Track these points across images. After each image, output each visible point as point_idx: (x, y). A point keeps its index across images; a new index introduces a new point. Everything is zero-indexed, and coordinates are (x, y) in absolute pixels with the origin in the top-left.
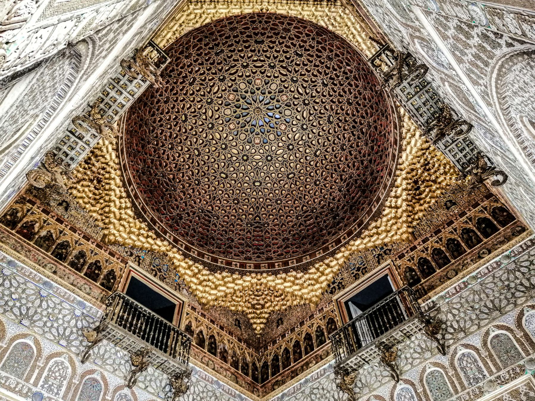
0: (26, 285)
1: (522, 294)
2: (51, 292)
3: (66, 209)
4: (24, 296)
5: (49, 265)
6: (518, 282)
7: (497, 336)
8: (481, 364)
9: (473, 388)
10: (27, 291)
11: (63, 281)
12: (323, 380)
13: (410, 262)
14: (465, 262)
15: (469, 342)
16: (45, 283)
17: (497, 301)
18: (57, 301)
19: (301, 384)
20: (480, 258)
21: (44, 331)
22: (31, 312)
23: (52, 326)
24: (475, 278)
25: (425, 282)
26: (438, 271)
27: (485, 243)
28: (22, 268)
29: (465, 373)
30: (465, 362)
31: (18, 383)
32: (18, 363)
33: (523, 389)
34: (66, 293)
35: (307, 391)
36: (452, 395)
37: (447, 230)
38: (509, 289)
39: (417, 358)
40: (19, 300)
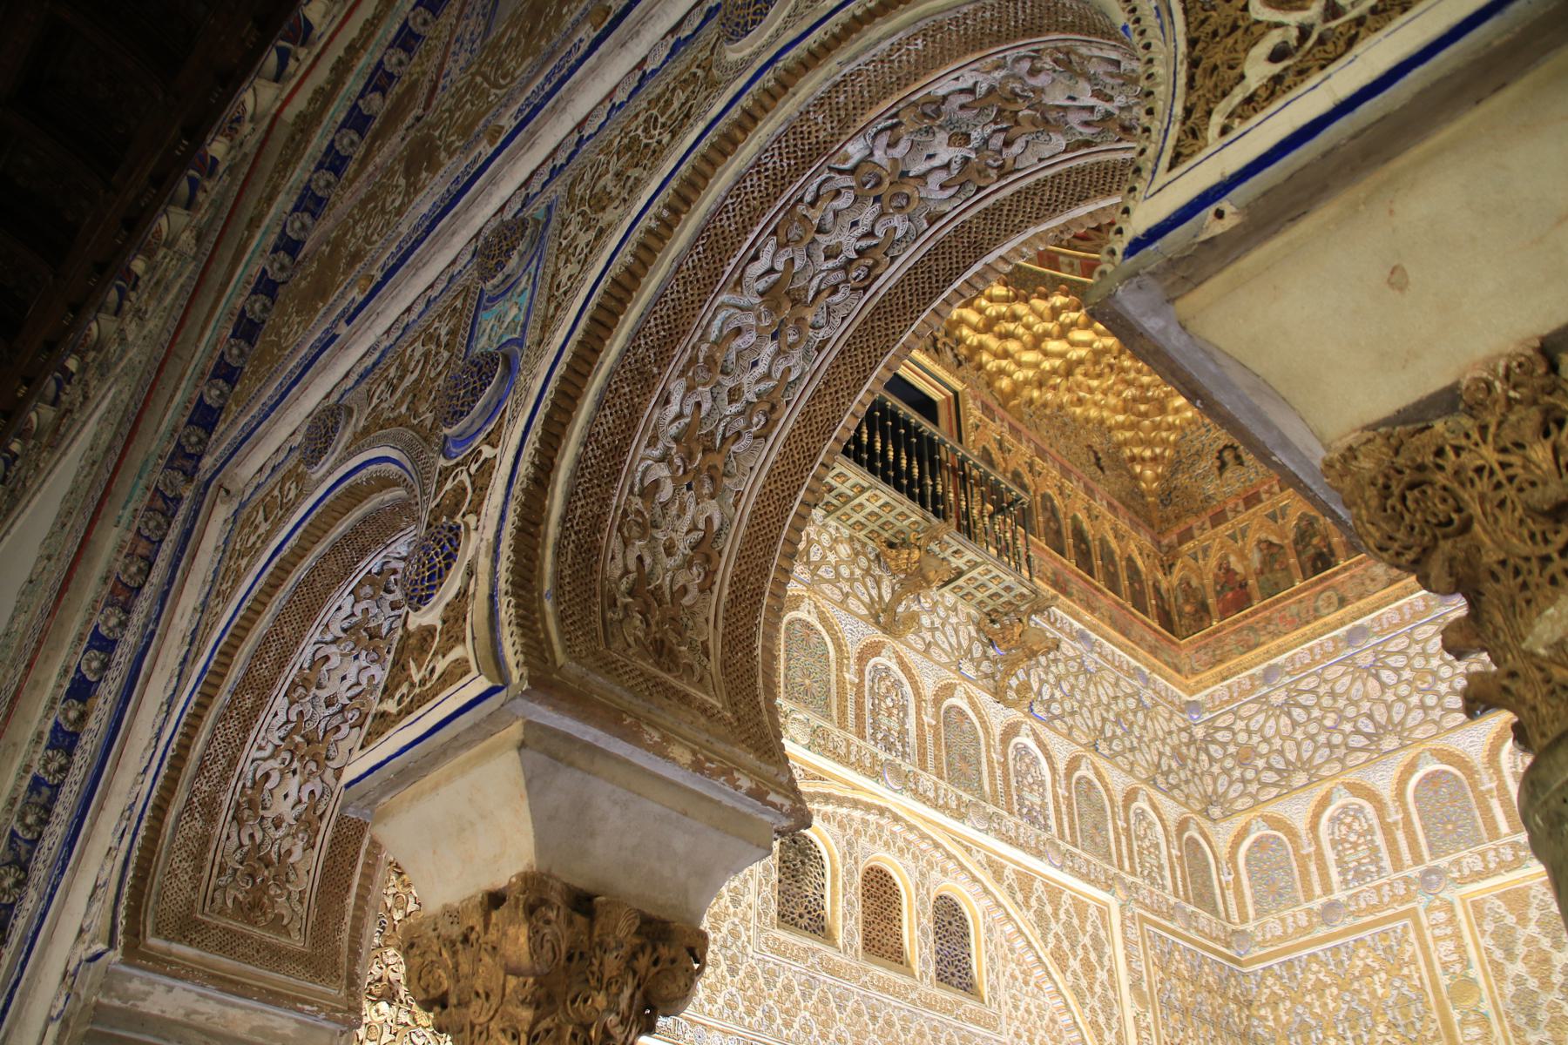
0: (1326, 681)
2: (1374, 640)
3: (1238, 458)
4: (1341, 703)
5: (1320, 603)
10: (1339, 688)
11: (1372, 599)
16: (1351, 638)
18: (1402, 642)
21: (1434, 722)
22: (1381, 717)
23: (1440, 697)
28: (1292, 660)
31: (1483, 854)
32: (1449, 821)
34: (1399, 609)
40: (1342, 718)
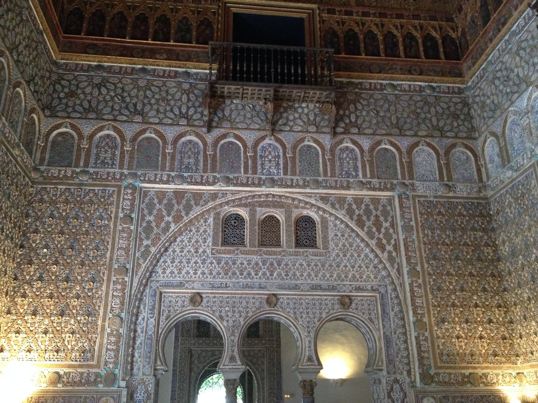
1: (426, 128)
6: (429, 116)
7: (386, 149)
8: (359, 165)
9: (343, 179)
12: (171, 83)
13: (339, 25)
14: (394, 66)
15: (358, 141)
17: (402, 121)
19: (133, 69)
20: (410, 72)
24: (394, 87)
25: (345, 58)
26: (364, 56)
27: (422, 62)
29: (341, 163)
30: (345, 155)
33: (384, 201)
35: (142, 83)
36: (319, 175)
37: (393, 21)
38: (417, 118)
39: (299, 125)
